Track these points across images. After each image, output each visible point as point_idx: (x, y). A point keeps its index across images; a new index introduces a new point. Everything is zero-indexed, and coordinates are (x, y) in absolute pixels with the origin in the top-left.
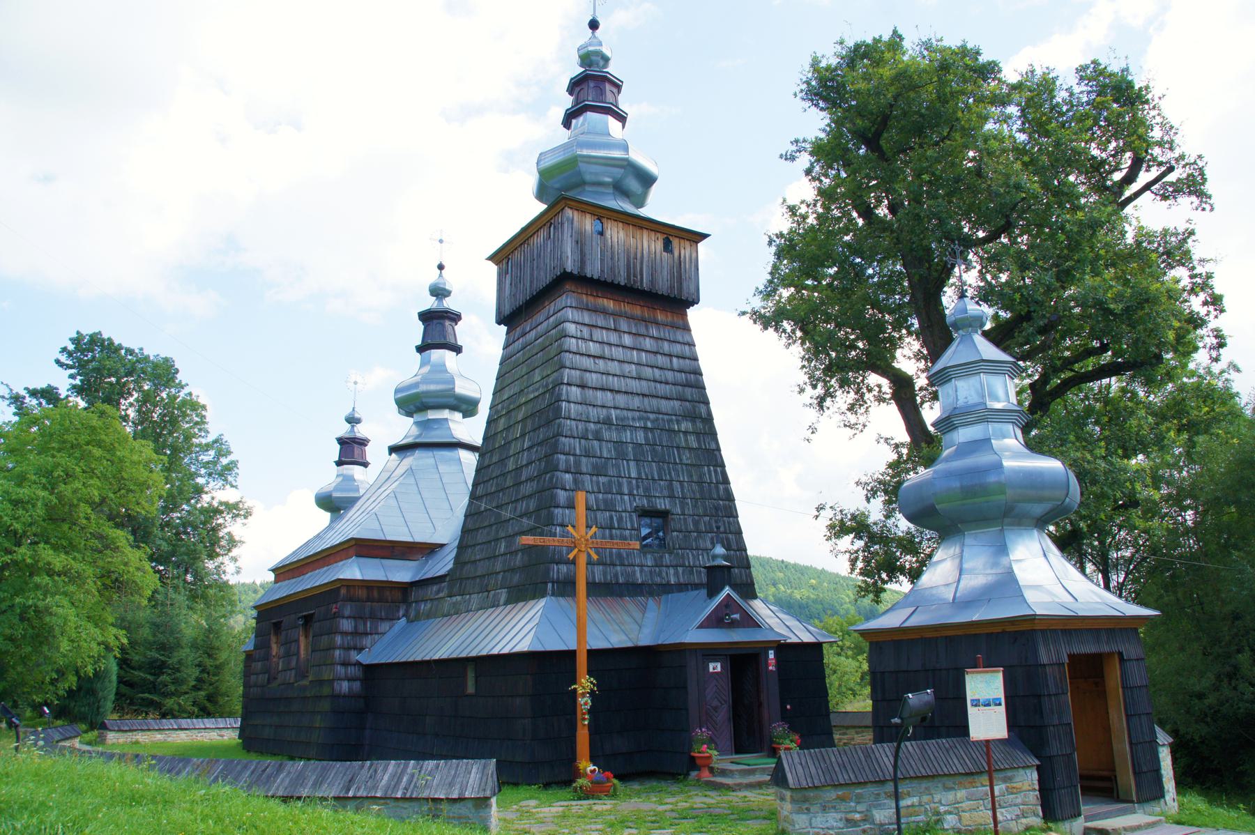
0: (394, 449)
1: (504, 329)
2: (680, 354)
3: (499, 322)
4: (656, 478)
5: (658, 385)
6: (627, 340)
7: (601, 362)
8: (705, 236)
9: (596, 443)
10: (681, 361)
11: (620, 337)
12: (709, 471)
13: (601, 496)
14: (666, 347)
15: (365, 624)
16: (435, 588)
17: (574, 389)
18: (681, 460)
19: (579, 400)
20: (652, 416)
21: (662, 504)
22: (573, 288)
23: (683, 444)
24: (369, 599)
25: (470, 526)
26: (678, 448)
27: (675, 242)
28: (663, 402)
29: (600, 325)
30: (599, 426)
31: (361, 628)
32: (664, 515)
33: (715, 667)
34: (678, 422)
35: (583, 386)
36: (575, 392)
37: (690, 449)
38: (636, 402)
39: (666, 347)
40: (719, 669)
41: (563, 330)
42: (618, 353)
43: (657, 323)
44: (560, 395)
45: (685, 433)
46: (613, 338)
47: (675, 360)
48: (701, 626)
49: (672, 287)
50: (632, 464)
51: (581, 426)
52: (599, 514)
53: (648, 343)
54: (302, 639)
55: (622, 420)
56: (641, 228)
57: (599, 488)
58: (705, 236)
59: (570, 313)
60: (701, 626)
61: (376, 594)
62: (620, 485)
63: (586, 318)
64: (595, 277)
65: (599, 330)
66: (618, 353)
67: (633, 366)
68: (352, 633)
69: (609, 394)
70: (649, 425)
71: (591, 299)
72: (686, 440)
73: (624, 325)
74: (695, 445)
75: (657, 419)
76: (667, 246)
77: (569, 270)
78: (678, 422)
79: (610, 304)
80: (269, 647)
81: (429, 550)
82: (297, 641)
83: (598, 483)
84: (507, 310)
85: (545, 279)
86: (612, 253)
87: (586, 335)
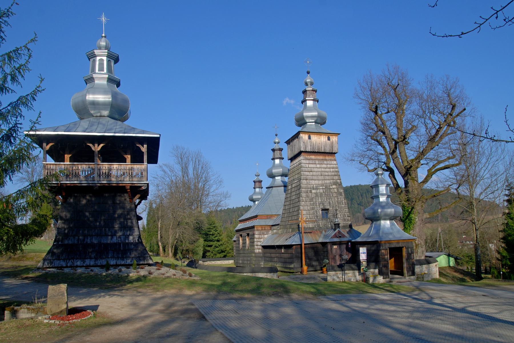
0: (267, 188)
2: (333, 167)
4: (326, 201)
6: (318, 166)
7: (311, 173)
9: (310, 194)
10: (333, 169)
12: (340, 198)
13: (311, 207)
14: (329, 166)
15: (261, 236)
16: (277, 227)
18: (332, 195)
20: (325, 185)
21: (327, 207)
22: (304, 155)
23: (333, 191)
24: (262, 230)
25: (284, 212)
27: (331, 137)
28: (328, 181)
29: (311, 163)
31: (260, 237)
32: (328, 210)
33: (335, 247)
34: (332, 186)
37: (335, 192)
38: (320, 182)
39: (329, 166)
40: (336, 247)
41: (301, 166)
42: (316, 170)
43: (326, 160)
45: (334, 188)
46: (314, 166)
47: (331, 169)
49: (330, 150)
50: (319, 198)
51: (306, 190)
52: (311, 211)
53: (324, 166)
55: (317, 187)
56: (321, 135)
57: (311, 205)
59: (303, 161)
60: (332, 238)
61: (263, 229)
62: (316, 203)
63: (307, 162)
64: (309, 151)
65: (311, 165)
68: (258, 238)
69: (313, 181)
70: (324, 187)
71: (309, 156)
72: (334, 190)
73: (317, 162)
74: (336, 191)
75: (326, 185)
76: (329, 139)
77: (302, 150)
78: (332, 186)
79: (313, 157)
80: (239, 241)
82: (246, 240)
83: (311, 203)
85: (296, 152)
86: (314, 144)
87: (307, 166)
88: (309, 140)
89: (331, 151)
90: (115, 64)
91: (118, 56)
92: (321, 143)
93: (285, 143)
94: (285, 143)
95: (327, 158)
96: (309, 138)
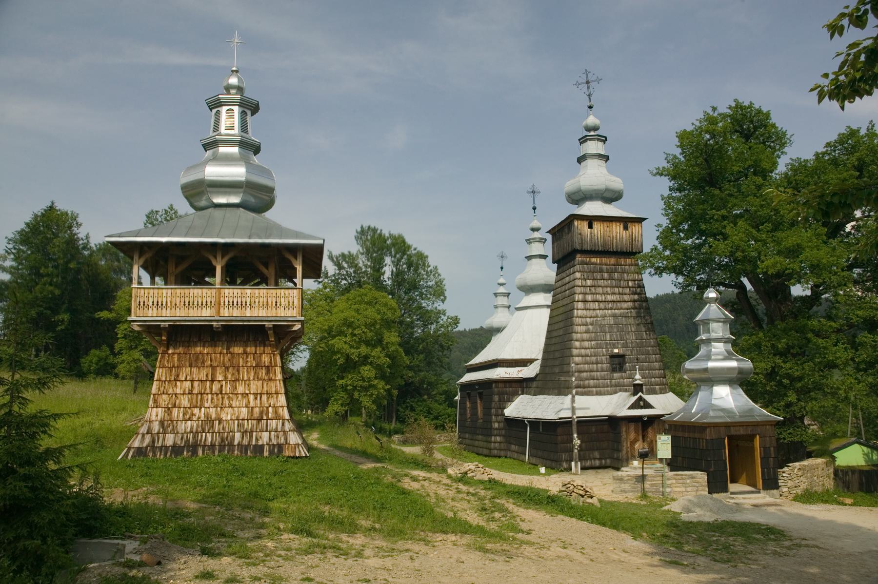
1: (556, 265)
3: (554, 262)
5: (621, 296)
6: (606, 275)
7: (593, 289)
8: (645, 219)
11: (603, 276)
13: (592, 350)
17: (580, 303)
19: (583, 307)
26: (630, 324)
30: (592, 319)
35: (584, 301)
36: (580, 305)
44: (574, 306)
46: (598, 275)
48: (629, 408)
54: (479, 401)
58: (645, 219)
60: (629, 408)
66: (602, 283)
67: (609, 288)
81: (531, 361)
84: (557, 259)
88: (589, 230)
89: (629, 250)
90: (252, 115)
91: (258, 104)
92: (611, 236)
93: (547, 232)
94: (547, 232)
95: (622, 261)
96: (590, 227)
